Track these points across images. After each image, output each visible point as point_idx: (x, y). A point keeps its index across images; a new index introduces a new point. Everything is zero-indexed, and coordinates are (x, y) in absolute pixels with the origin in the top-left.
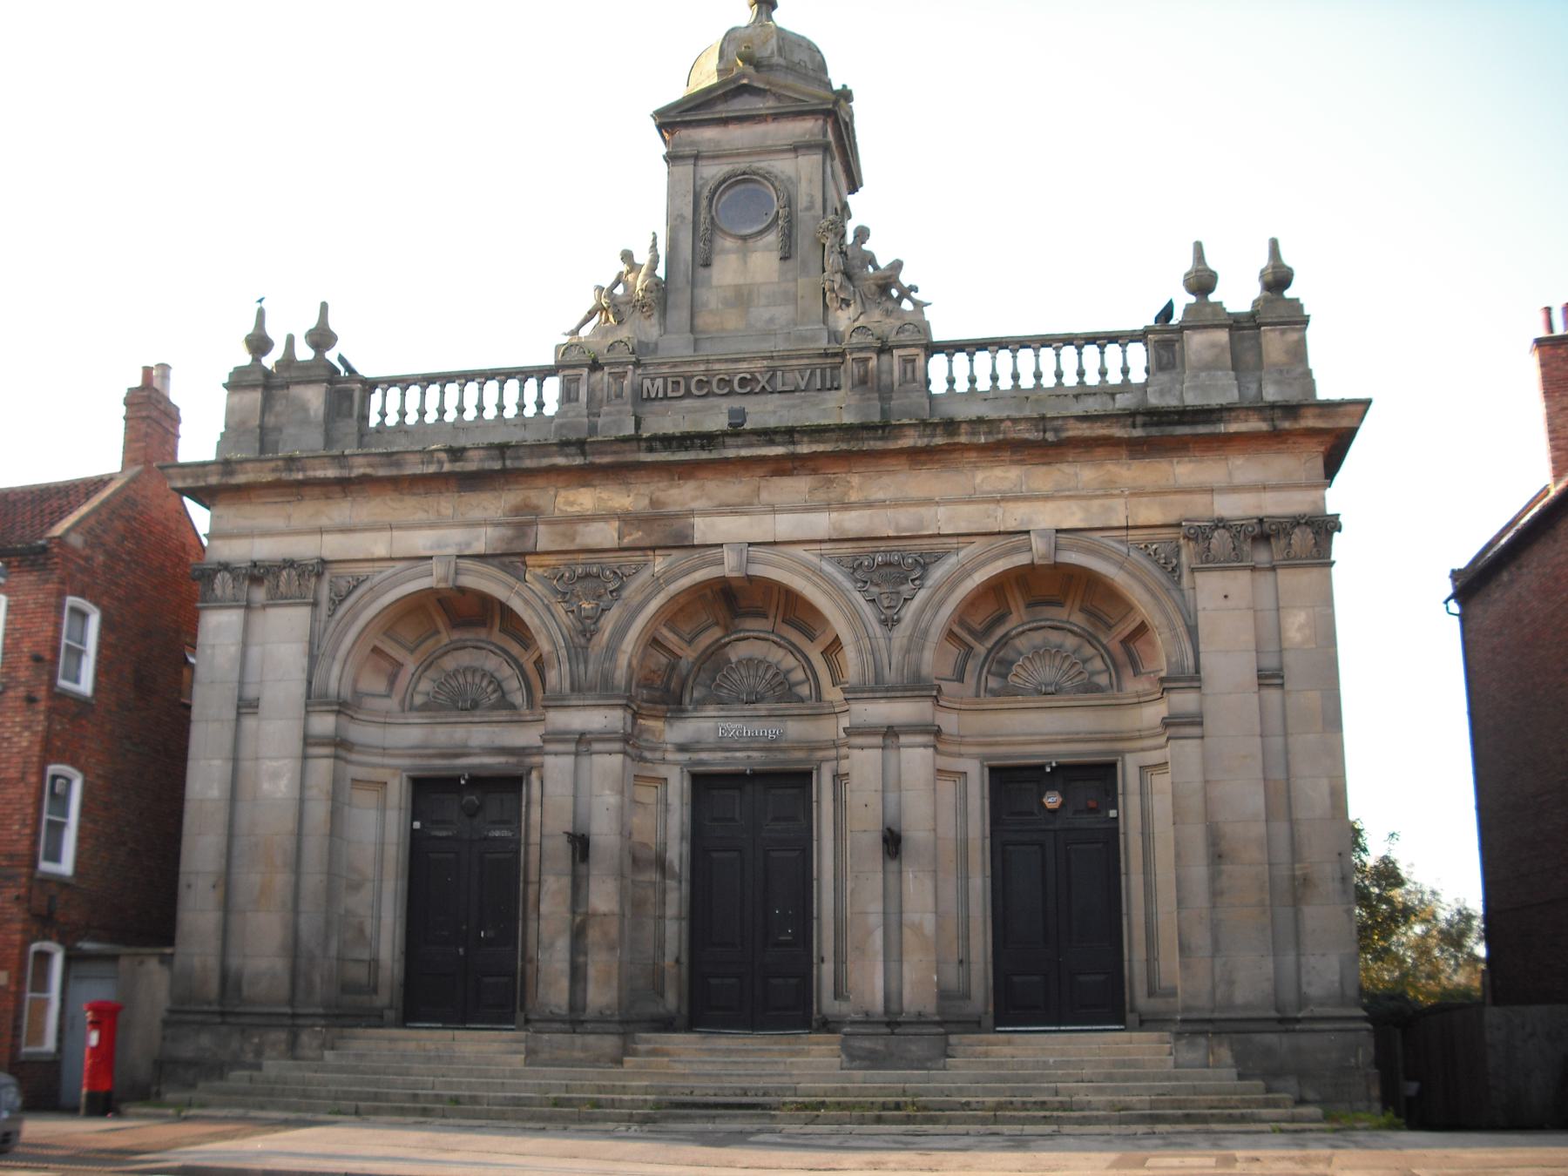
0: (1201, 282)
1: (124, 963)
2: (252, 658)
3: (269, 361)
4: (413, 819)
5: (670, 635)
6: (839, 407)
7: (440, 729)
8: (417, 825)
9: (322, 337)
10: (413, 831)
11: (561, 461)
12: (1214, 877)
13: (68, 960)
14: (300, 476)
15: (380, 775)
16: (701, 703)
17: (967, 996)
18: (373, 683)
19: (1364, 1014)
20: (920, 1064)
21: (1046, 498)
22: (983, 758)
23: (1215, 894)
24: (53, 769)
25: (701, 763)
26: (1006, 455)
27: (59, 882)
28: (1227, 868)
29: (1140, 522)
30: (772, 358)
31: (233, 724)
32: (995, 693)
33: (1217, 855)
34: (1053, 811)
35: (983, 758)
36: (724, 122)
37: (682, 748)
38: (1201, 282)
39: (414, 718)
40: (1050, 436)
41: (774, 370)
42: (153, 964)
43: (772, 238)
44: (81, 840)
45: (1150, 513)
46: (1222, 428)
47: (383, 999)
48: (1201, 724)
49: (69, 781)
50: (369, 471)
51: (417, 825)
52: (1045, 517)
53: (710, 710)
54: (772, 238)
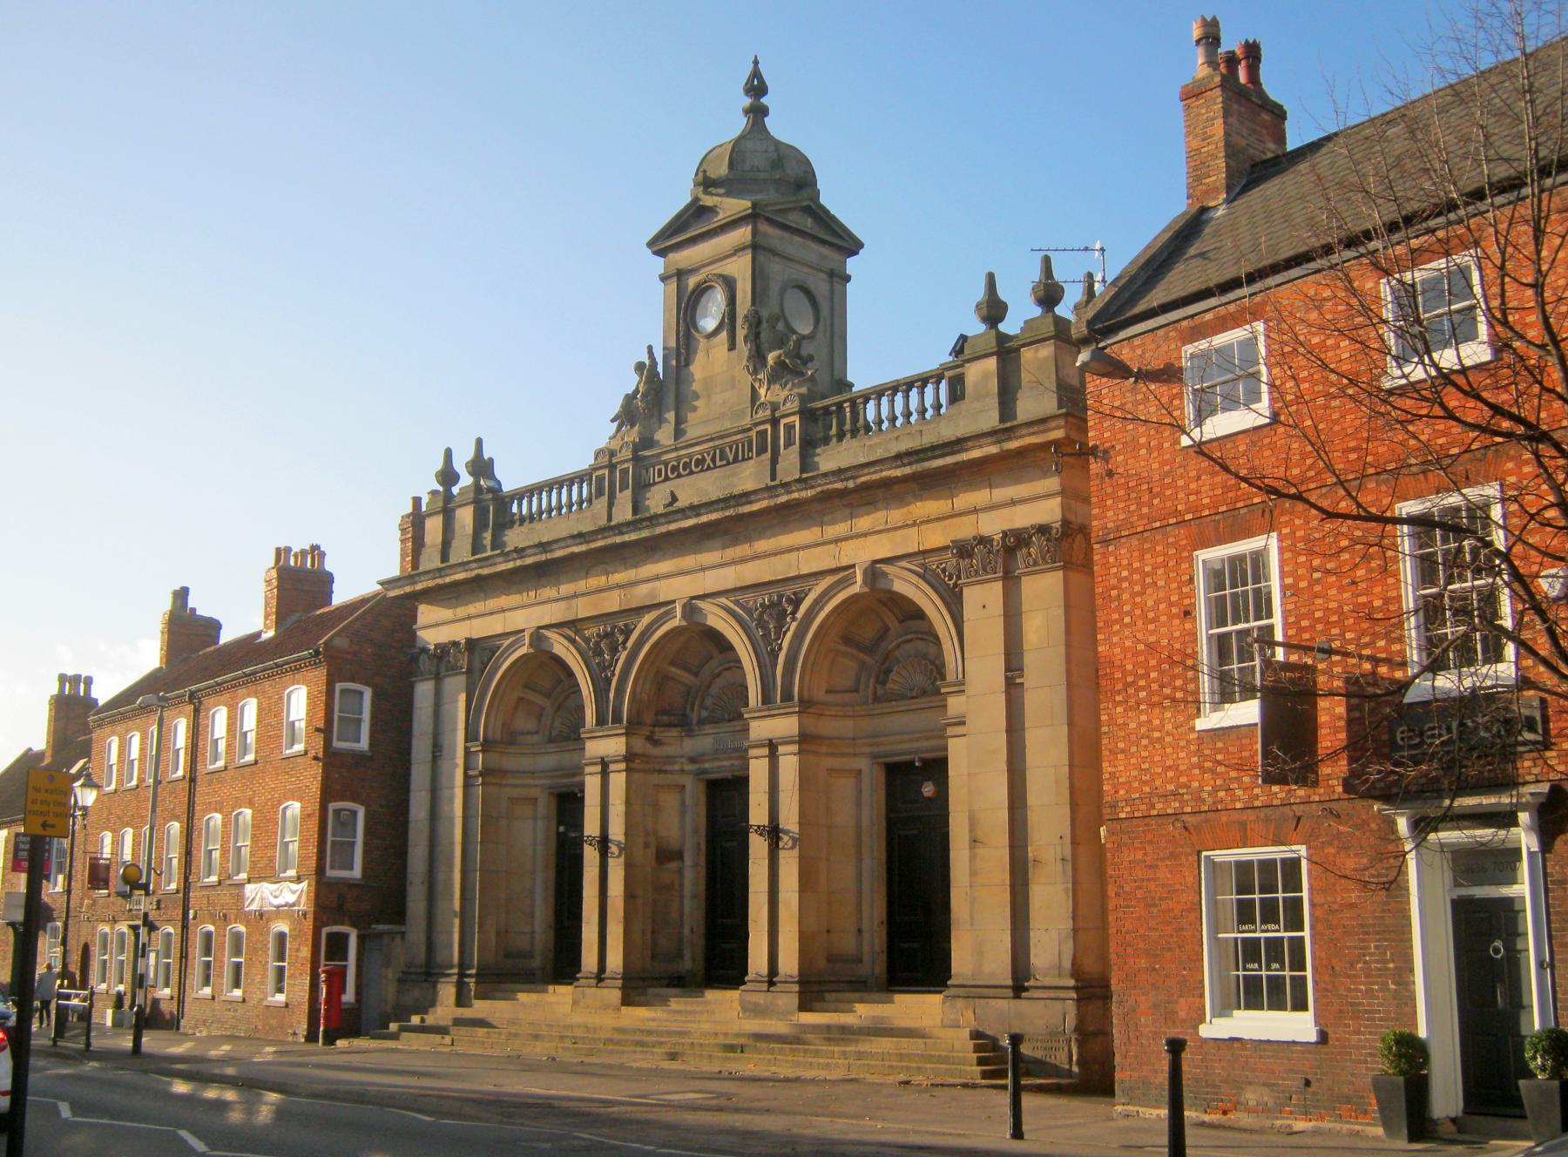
0: (993, 310)
1: (386, 939)
2: (451, 716)
3: (455, 490)
4: (559, 823)
5: (674, 670)
6: (749, 476)
7: (567, 756)
8: (562, 829)
9: (481, 466)
10: (558, 834)
11: (576, 549)
12: (972, 859)
13: (362, 939)
14: (448, 580)
15: (534, 792)
16: (701, 722)
17: (860, 961)
18: (523, 723)
19: (1072, 983)
20: (783, 1015)
21: (865, 535)
22: (875, 756)
23: (973, 874)
24: (332, 806)
25: (704, 772)
26: (837, 502)
27: (349, 885)
28: (981, 851)
29: (928, 546)
30: (712, 440)
31: (429, 765)
32: (877, 699)
33: (974, 841)
34: (929, 799)
35: (875, 756)
36: (693, 241)
37: (693, 760)
38: (993, 310)
39: (551, 748)
40: (851, 484)
41: (715, 448)
42: (398, 939)
43: (724, 334)
44: (366, 852)
45: (936, 537)
46: (965, 456)
47: (536, 963)
48: (963, 723)
49: (355, 813)
50: (481, 571)
51: (562, 829)
52: (861, 553)
53: (708, 729)
54: (724, 334)
